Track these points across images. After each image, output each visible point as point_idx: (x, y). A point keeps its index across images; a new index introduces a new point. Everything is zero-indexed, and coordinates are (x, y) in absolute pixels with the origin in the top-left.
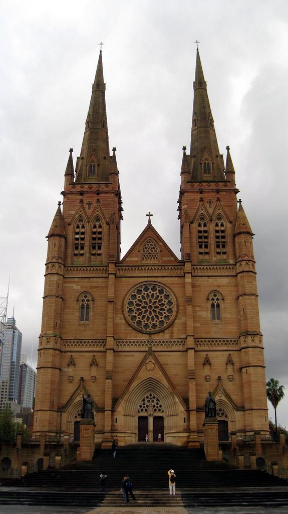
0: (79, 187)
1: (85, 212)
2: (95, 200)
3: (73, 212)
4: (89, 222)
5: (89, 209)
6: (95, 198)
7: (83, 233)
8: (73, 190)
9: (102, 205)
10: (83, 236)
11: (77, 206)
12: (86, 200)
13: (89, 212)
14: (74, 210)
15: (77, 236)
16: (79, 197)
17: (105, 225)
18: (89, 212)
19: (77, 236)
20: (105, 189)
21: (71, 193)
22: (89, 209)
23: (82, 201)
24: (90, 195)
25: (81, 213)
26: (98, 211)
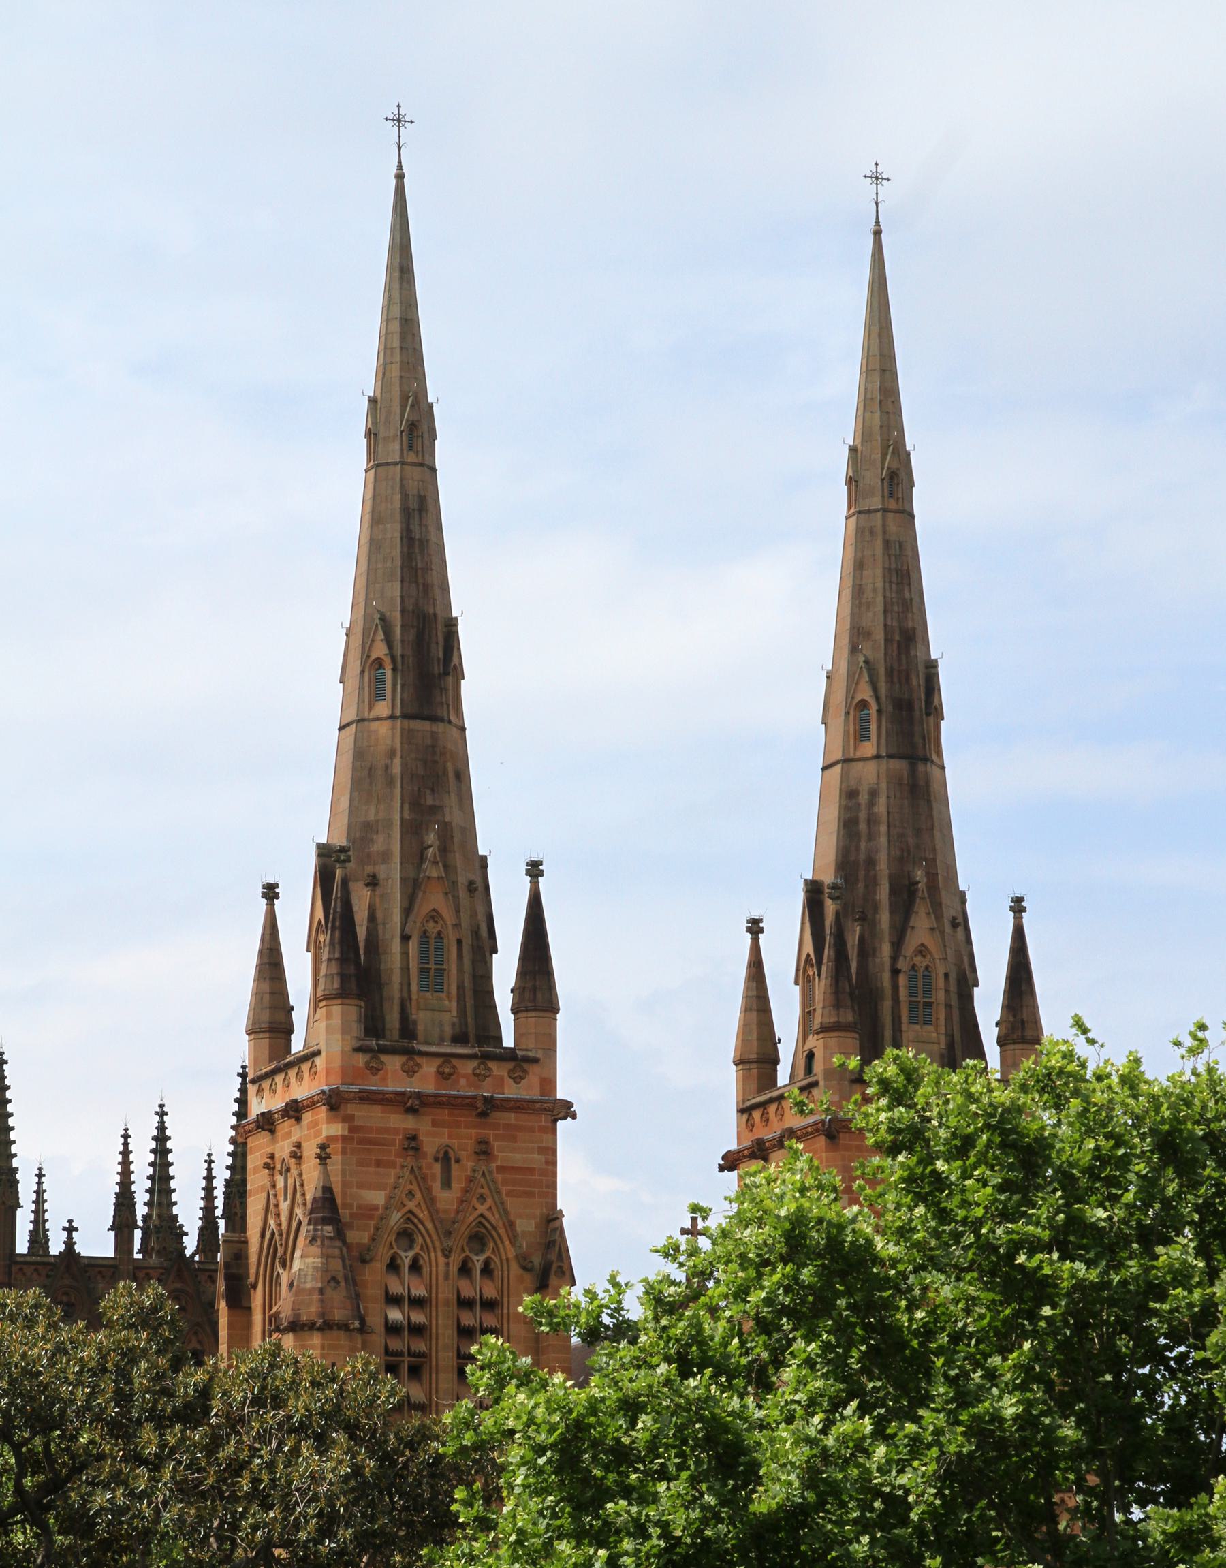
0: (398, 1066)
1: (430, 1201)
2: (470, 1145)
3: (378, 1198)
4: (447, 1253)
5: (447, 1184)
6: (463, 1138)
7: (417, 1303)
8: (373, 1085)
9: (501, 1169)
10: (418, 1317)
11: (392, 1165)
12: (431, 1144)
13: (446, 1198)
14: (379, 1187)
15: (395, 1315)
16: (400, 1122)
17: (514, 1267)
18: (446, 1198)
19: (395, 1315)
20: (511, 1091)
21: (367, 1098)
22: (447, 1184)
23: (412, 1143)
24: (444, 1115)
25: (411, 1205)
26: (482, 1198)
